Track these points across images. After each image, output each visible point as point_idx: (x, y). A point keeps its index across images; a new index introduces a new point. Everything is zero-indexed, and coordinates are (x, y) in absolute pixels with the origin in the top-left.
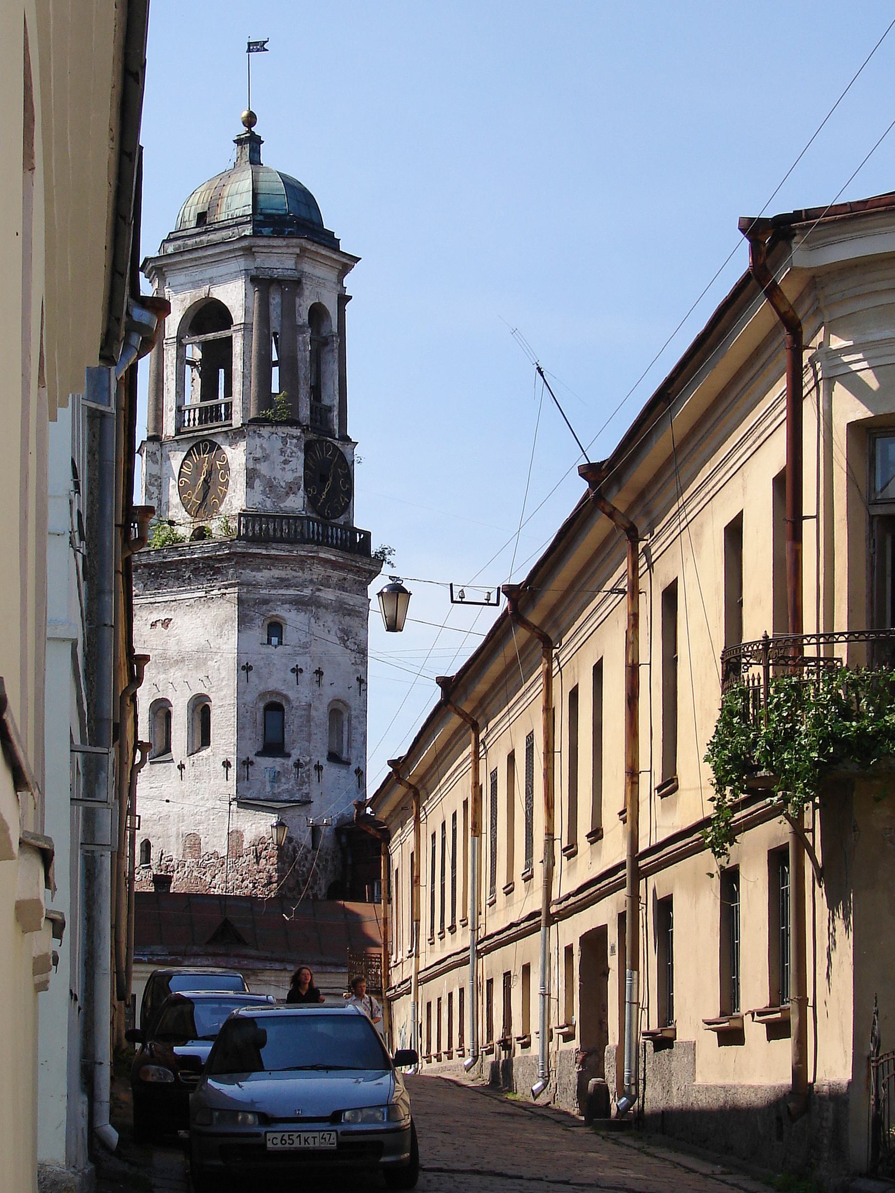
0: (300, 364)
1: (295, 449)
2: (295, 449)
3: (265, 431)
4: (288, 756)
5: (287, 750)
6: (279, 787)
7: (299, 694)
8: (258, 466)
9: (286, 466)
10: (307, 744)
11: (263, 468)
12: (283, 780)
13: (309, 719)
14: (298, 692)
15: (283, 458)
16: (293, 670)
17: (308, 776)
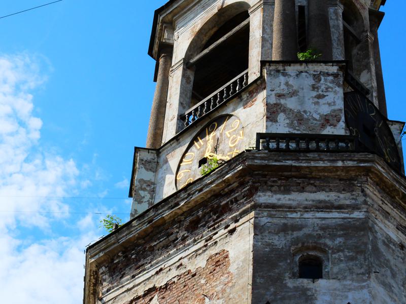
0: (332, 30)
1: (331, 85)
2: (331, 85)
8: (282, 101)
9: (320, 101)
11: (291, 103)
15: (314, 94)
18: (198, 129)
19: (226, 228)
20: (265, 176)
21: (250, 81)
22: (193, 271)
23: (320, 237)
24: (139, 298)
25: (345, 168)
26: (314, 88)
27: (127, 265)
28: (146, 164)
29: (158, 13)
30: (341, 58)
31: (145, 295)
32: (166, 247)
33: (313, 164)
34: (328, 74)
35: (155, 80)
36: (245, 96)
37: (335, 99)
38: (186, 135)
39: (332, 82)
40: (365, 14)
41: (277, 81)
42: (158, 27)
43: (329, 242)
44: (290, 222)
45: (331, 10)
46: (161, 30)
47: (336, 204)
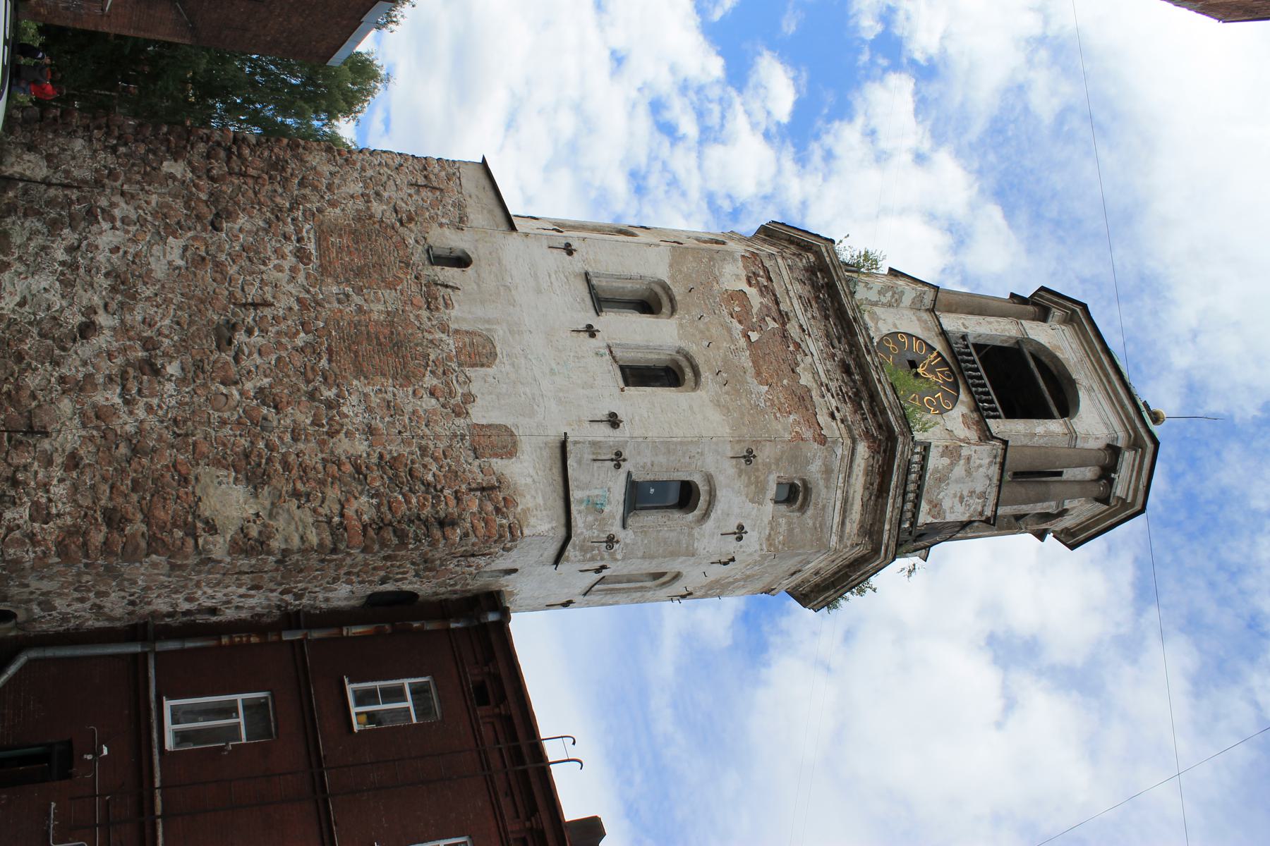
3: (995, 470)
4: (624, 527)
5: (630, 521)
6: (580, 512)
7: (709, 537)
8: (962, 462)
10: (640, 554)
11: (959, 470)
12: (590, 518)
13: (674, 554)
14: (712, 535)
15: (965, 493)
16: (741, 527)
17: (593, 559)
18: (949, 360)
19: (837, 409)
20: (885, 452)
21: (990, 422)
22: (798, 370)
23: (816, 504)
24: (777, 303)
25: (881, 532)
26: (972, 493)
27: (813, 286)
28: (920, 297)
29: (1084, 307)
30: (1000, 512)
31: (780, 311)
32: (828, 336)
33: (890, 501)
34: (984, 506)
35: (1013, 295)
36: (975, 415)
37: (955, 513)
38: (944, 344)
39: (975, 510)
40: (1044, 526)
41: (985, 455)
42: (1069, 304)
43: (810, 512)
44: (834, 476)
45: (1053, 503)
46: (1065, 307)
47: (847, 521)
